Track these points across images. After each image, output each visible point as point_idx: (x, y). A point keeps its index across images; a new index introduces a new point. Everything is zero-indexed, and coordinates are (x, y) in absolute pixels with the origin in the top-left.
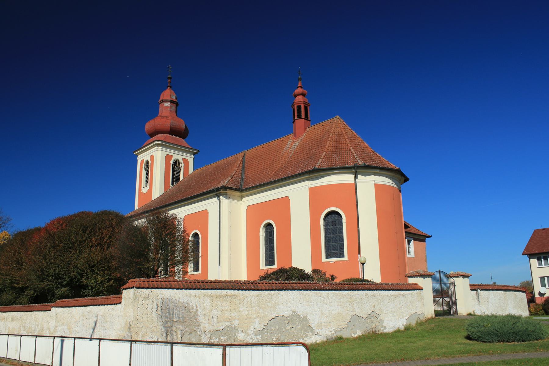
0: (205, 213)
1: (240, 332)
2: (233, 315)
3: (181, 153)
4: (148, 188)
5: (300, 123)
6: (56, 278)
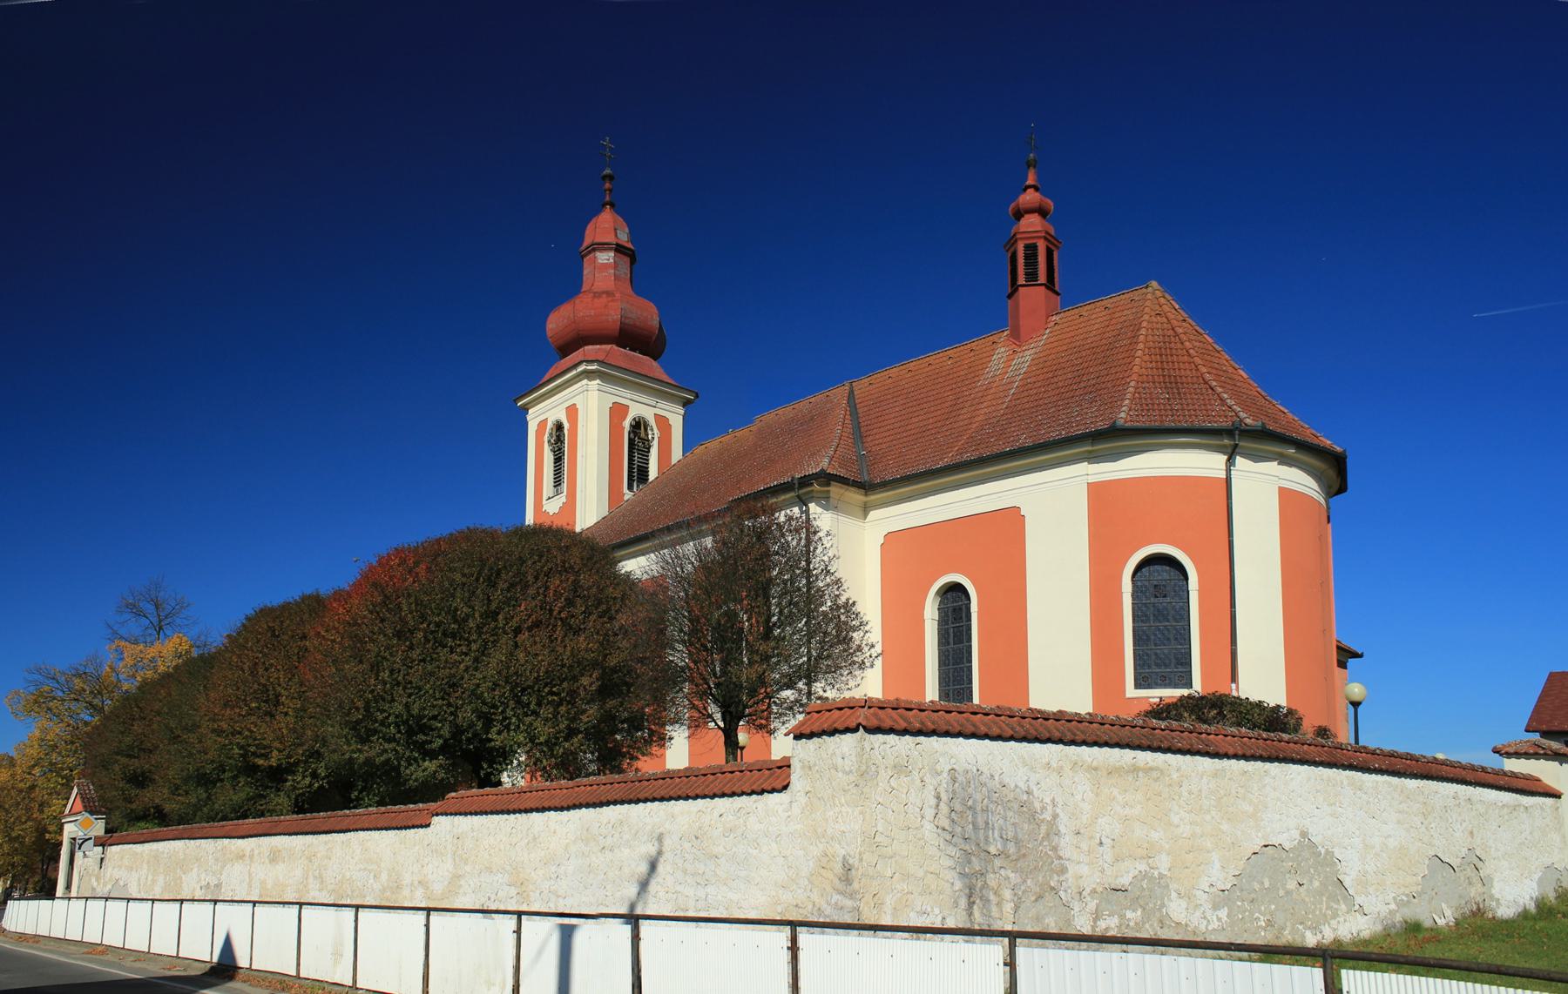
1: (1174, 895)
2: (1155, 835)
4: (562, 499)
6: (410, 733)
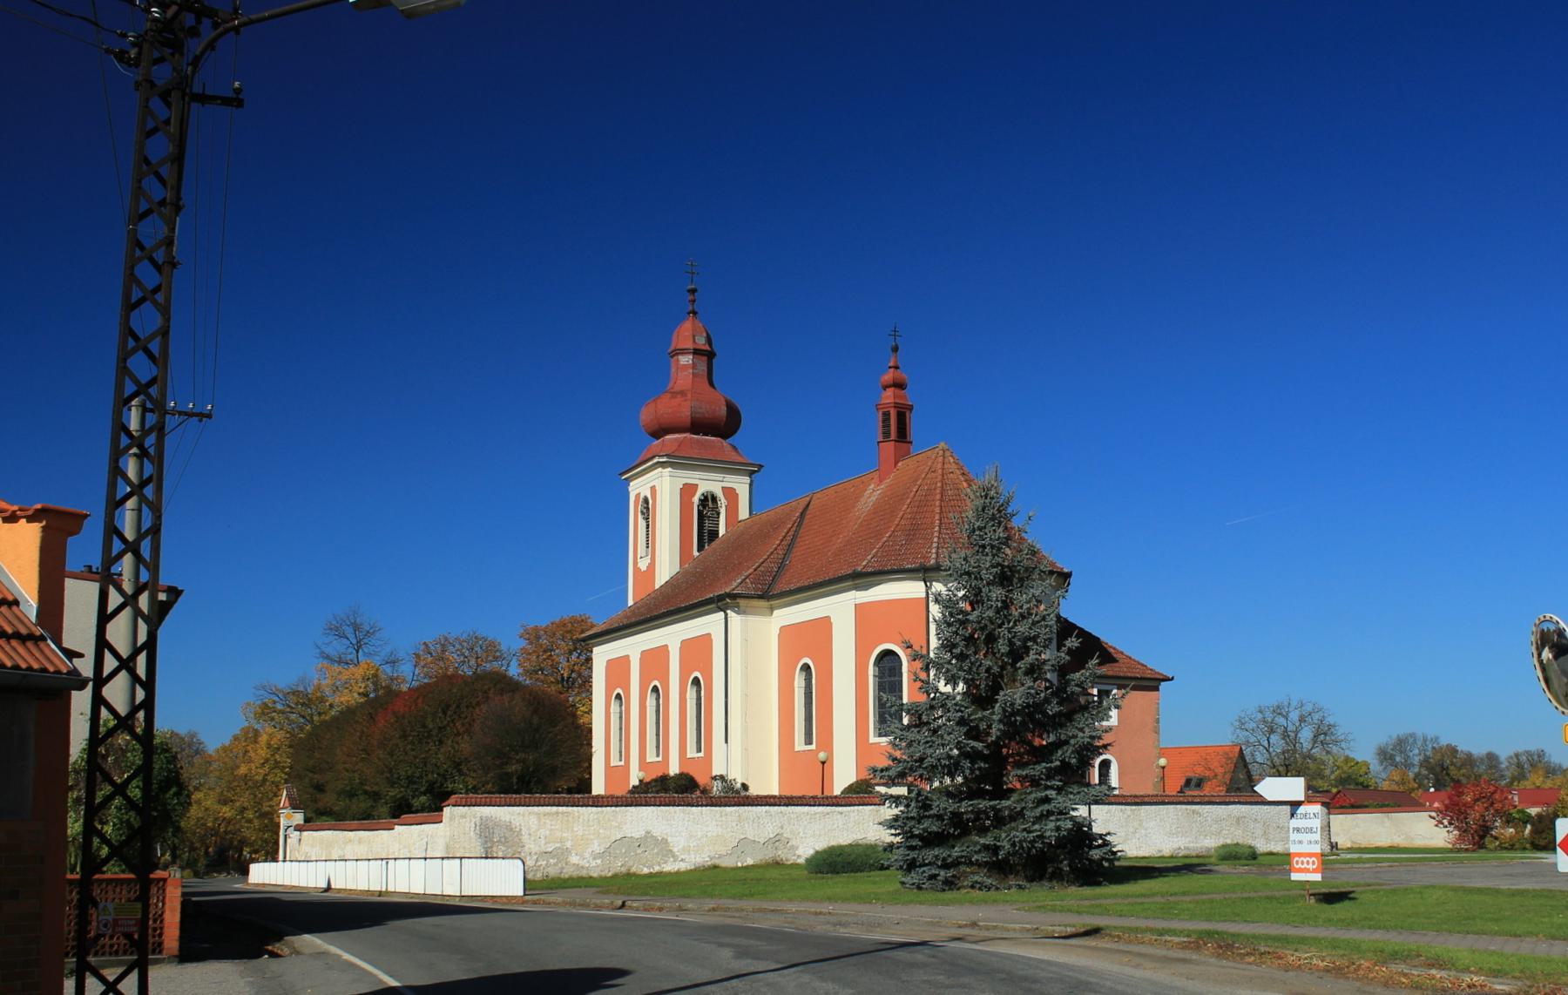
0: (706, 640)
3: (719, 476)
4: (647, 561)
5: (889, 447)
